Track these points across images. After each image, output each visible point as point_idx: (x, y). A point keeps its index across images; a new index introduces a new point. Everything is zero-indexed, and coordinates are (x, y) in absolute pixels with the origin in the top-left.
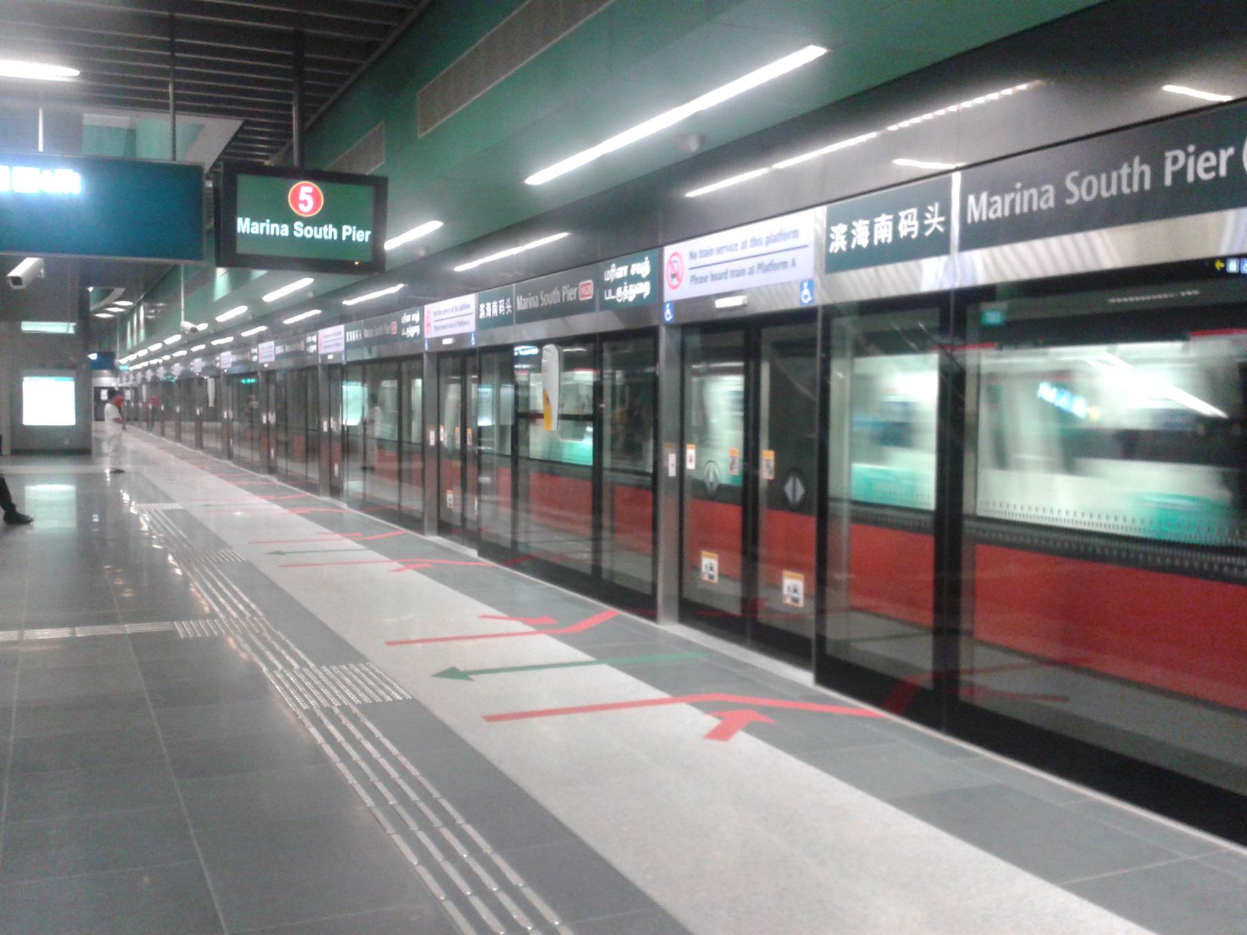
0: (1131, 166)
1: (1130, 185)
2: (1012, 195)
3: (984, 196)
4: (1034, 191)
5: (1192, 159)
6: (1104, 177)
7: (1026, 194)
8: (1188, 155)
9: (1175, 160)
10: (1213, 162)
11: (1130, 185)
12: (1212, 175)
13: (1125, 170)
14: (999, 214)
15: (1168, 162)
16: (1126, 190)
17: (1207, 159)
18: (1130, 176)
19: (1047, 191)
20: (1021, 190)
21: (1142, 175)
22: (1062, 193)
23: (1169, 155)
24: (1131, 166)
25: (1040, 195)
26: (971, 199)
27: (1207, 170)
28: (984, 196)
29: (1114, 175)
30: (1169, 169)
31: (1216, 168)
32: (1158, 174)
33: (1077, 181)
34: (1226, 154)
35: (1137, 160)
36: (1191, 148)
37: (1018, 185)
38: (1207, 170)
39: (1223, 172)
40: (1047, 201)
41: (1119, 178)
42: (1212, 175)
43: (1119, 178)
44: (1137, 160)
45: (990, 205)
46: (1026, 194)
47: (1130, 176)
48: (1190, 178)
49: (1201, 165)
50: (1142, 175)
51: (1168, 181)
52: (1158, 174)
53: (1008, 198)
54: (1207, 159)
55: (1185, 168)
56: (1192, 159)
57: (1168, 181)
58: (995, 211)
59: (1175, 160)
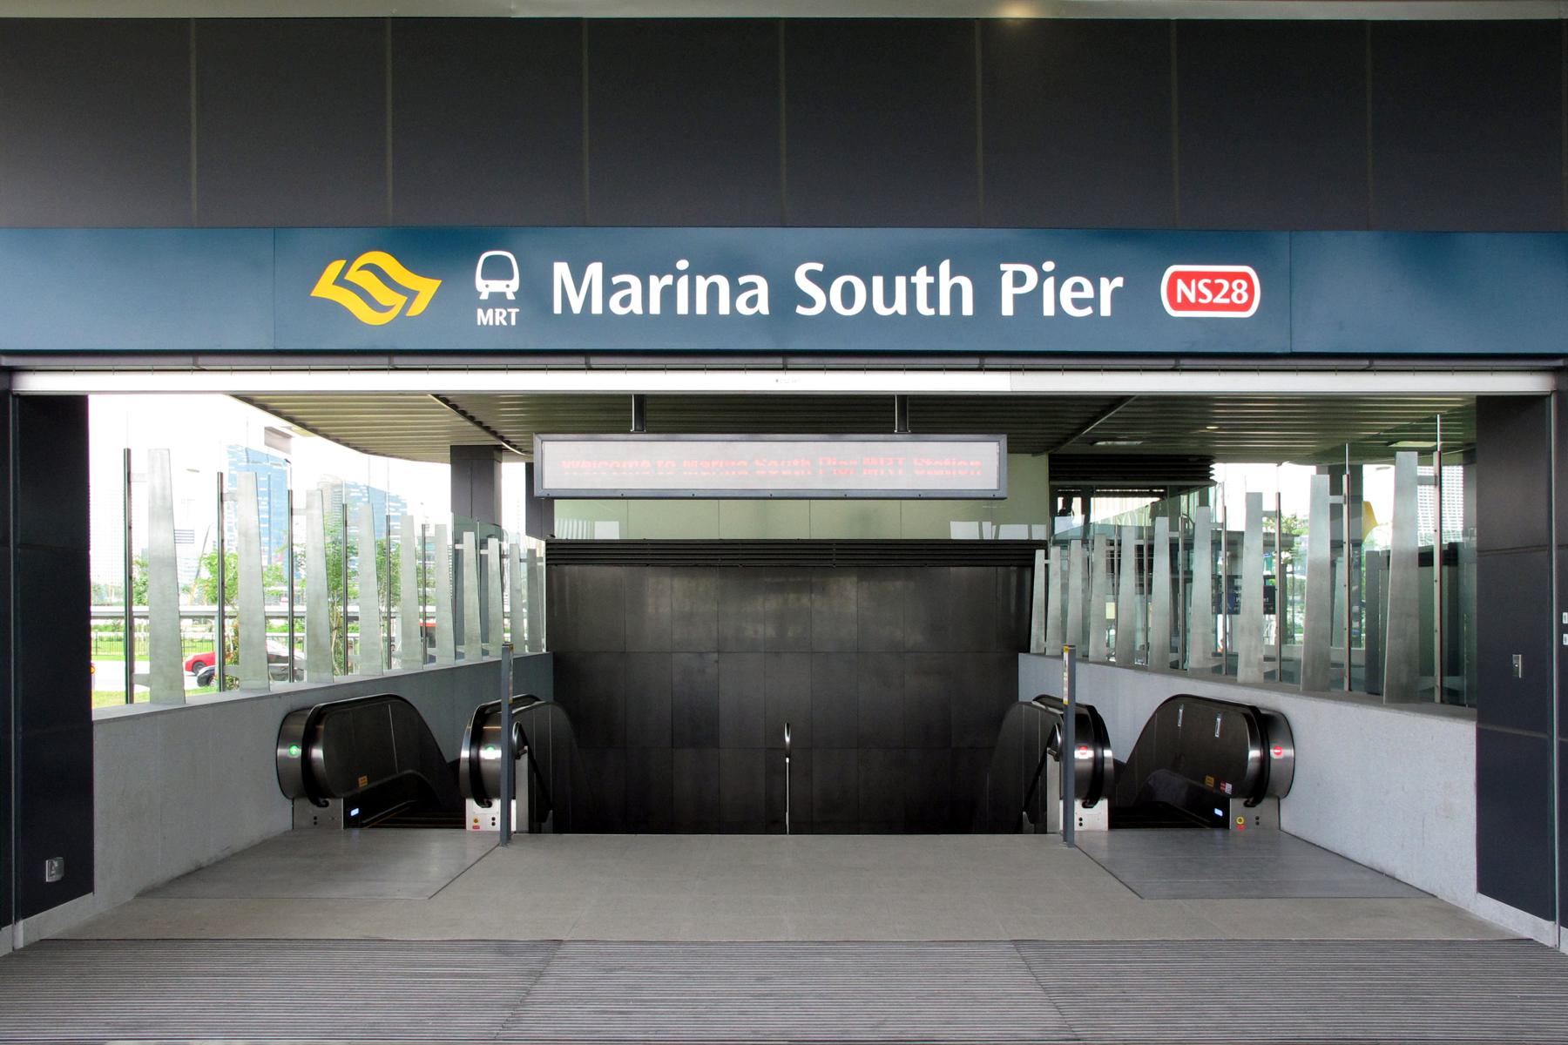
0: (933, 271)
1: (933, 299)
2: (668, 280)
3: (595, 271)
5: (1049, 284)
6: (878, 282)
7: (702, 284)
8: (1043, 276)
9: (1019, 279)
10: (1089, 292)
11: (933, 299)
12: (1088, 311)
13: (922, 278)
14: (636, 307)
15: (1007, 280)
18: (933, 290)
20: (692, 273)
21: (956, 291)
22: (786, 295)
23: (1009, 269)
24: (933, 271)
25: (736, 290)
26: (561, 270)
27: (1078, 303)
28: (595, 271)
29: (900, 282)
31: (1095, 302)
33: (823, 281)
35: (945, 267)
36: (1049, 266)
37: (683, 265)
39: (1106, 310)
40: (752, 302)
41: (911, 290)
42: (1088, 311)
43: (911, 290)
44: (945, 267)
45: (609, 290)
46: (702, 284)
47: (933, 290)
48: (1049, 310)
50: (956, 291)
51: (1007, 309)
52: (988, 294)
53: (656, 285)
54: (1078, 287)
55: (1039, 289)
56: (1049, 284)
57: (1007, 309)
58: (625, 301)
59: (1019, 279)
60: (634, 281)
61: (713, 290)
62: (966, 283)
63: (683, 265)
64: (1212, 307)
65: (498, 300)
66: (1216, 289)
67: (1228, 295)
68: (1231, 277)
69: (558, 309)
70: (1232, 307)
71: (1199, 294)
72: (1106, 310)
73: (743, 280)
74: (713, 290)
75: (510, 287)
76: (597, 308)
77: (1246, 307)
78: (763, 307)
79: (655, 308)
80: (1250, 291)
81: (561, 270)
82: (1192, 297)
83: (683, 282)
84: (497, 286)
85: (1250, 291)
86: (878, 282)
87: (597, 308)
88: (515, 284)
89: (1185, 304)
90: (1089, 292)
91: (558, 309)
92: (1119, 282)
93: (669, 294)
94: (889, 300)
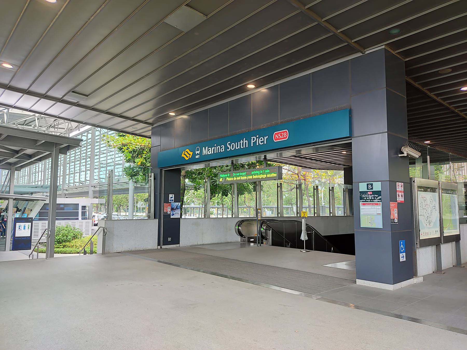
0: (243, 141)
1: (243, 146)
4: (219, 147)
9: (254, 139)
11: (243, 146)
13: (242, 142)
15: (252, 140)
16: (242, 147)
17: (261, 139)
18: (243, 143)
22: (226, 148)
23: (252, 138)
25: (221, 148)
26: (204, 148)
27: (261, 142)
30: (252, 142)
31: (264, 141)
32: (249, 143)
33: (230, 144)
34: (265, 138)
36: (258, 136)
38: (261, 142)
39: (265, 143)
46: (217, 147)
47: (243, 143)
48: (257, 144)
49: (260, 141)
51: (252, 145)
52: (249, 143)
54: (261, 139)
59: (254, 139)
60: (210, 148)
62: (247, 141)
66: (281, 135)
68: (283, 132)
71: (279, 137)
72: (265, 143)
75: (199, 152)
78: (223, 150)
80: (287, 134)
81: (204, 148)
85: (287, 134)
89: (277, 139)
92: (267, 137)
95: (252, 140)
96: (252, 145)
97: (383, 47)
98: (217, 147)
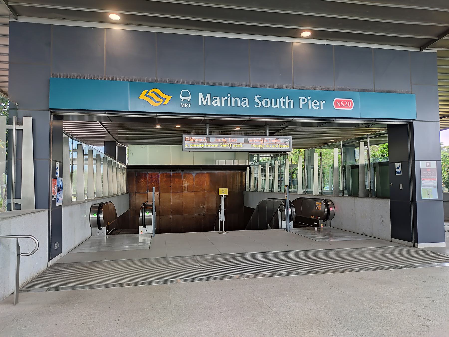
0: (285, 98)
1: (285, 105)
2: (226, 98)
3: (209, 95)
6: (273, 100)
8: (308, 100)
9: (303, 100)
11: (285, 105)
13: (282, 100)
15: (301, 100)
18: (285, 102)
19: (245, 100)
21: (290, 102)
22: (252, 102)
23: (301, 98)
24: (285, 98)
25: (241, 101)
26: (201, 95)
28: (209, 95)
29: (278, 100)
30: (301, 103)
31: (319, 106)
33: (261, 100)
40: (245, 104)
41: (280, 102)
43: (280, 102)
45: (212, 100)
46: (233, 99)
47: (285, 102)
49: (313, 104)
50: (290, 102)
51: (301, 107)
54: (316, 103)
58: (216, 103)
59: (303, 100)
61: (236, 101)
63: (229, 95)
64: (344, 107)
65: (186, 101)
66: (345, 104)
67: (347, 105)
68: (348, 101)
69: (200, 104)
70: (348, 107)
72: (322, 108)
73: (243, 99)
74: (236, 101)
76: (209, 104)
77: (351, 107)
78: (247, 105)
79: (223, 105)
81: (201, 95)
82: (340, 105)
83: (229, 99)
84: (186, 98)
86: (273, 100)
87: (209, 104)
88: (190, 98)
89: (338, 107)
90: (318, 104)
91: (200, 104)
92: (324, 102)
93: (226, 101)
94: (275, 104)
95: (301, 100)
96: (301, 107)
97: (436, 51)
98: (233, 99)
